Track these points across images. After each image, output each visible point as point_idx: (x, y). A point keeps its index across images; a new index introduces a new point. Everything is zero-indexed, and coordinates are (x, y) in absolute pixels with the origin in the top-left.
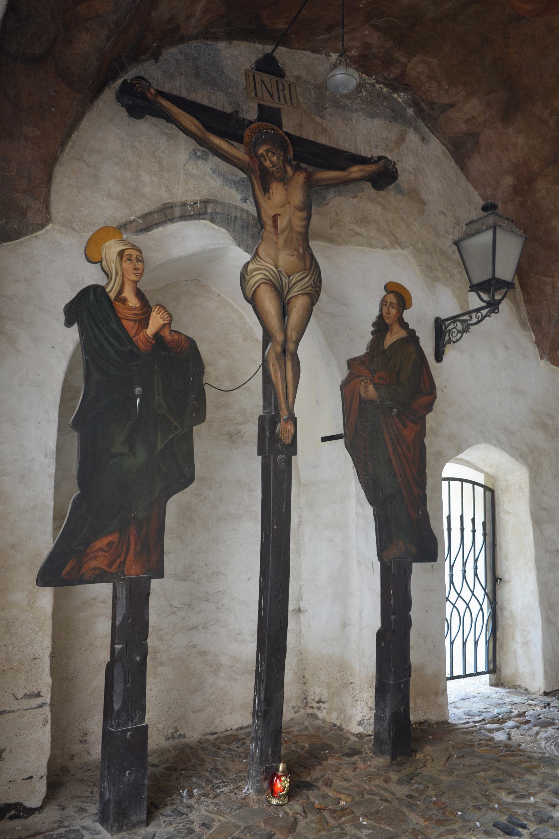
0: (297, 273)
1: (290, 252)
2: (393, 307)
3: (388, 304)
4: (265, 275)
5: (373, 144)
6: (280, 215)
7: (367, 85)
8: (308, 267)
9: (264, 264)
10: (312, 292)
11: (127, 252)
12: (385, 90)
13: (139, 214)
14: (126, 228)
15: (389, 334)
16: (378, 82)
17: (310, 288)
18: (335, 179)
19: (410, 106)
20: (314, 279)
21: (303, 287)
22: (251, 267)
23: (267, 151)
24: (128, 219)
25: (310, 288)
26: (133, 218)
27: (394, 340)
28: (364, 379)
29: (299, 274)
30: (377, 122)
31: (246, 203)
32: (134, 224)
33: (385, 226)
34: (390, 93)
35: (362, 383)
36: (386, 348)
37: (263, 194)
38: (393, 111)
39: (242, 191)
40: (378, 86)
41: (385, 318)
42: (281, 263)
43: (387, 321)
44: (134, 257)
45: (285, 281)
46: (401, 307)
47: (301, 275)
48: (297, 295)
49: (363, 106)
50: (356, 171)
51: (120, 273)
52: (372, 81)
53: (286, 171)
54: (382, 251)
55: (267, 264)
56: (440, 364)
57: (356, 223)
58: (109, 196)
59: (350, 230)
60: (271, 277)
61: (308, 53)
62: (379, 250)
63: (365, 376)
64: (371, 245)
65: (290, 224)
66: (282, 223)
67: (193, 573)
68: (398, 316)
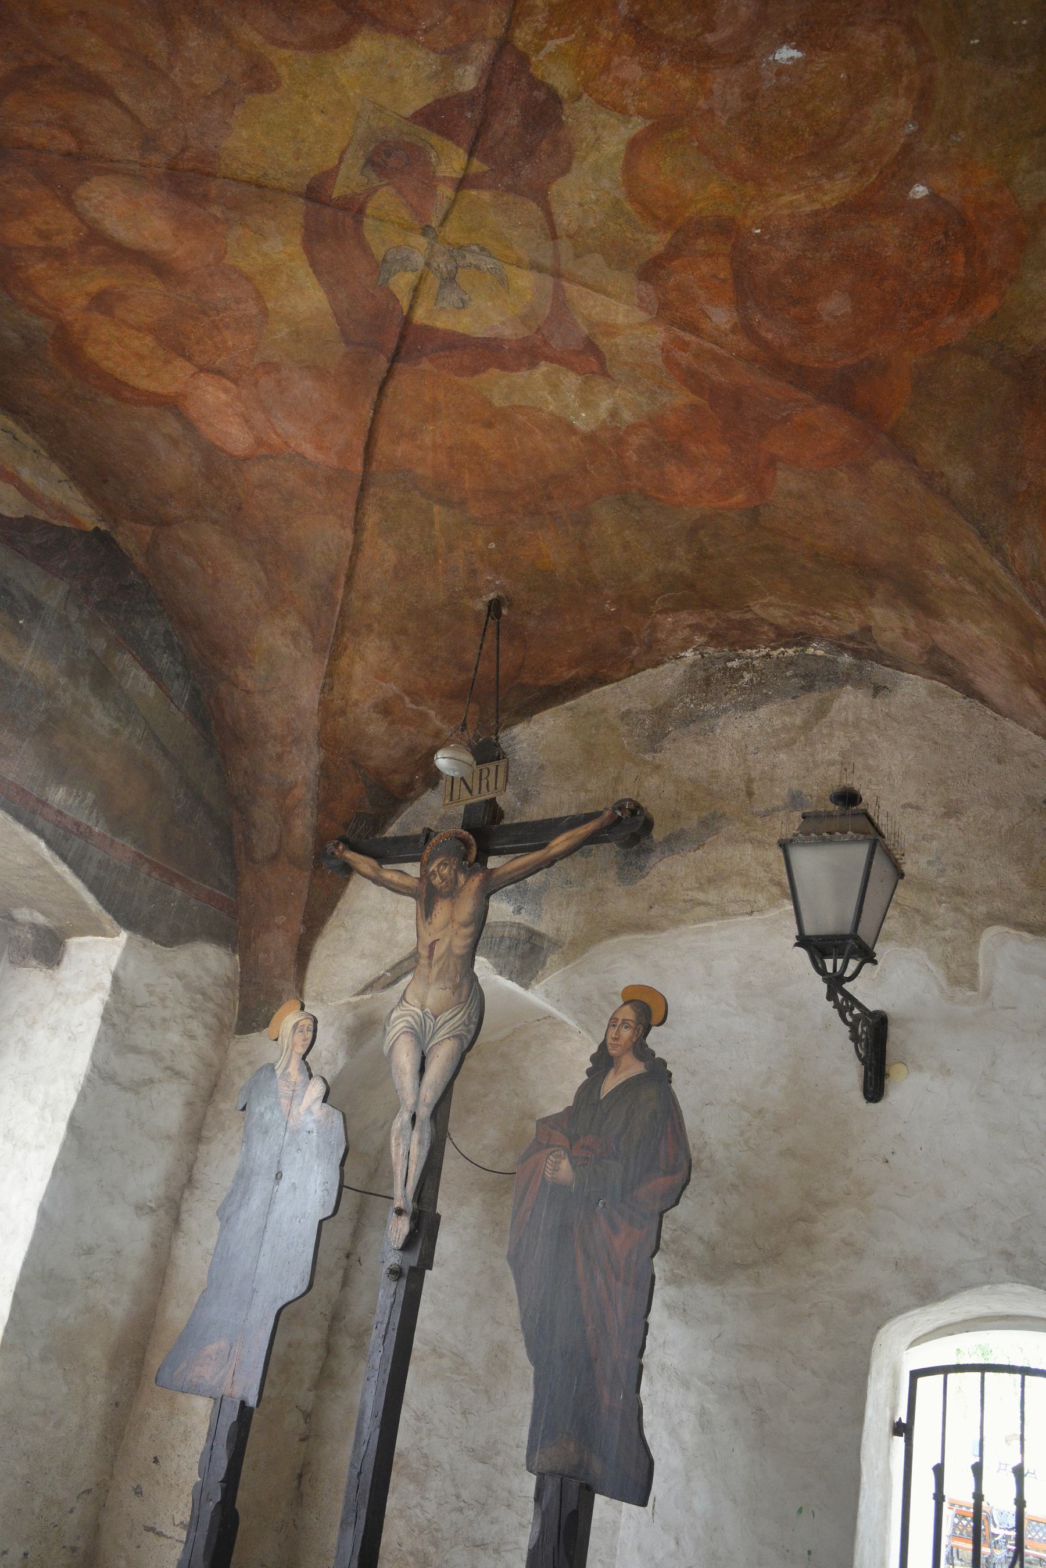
0: (447, 1010)
1: (442, 986)
2: (626, 1028)
3: (620, 1022)
4: (408, 1022)
5: (751, 749)
6: (438, 940)
7: (755, 662)
8: (463, 999)
9: (409, 1009)
10: (463, 1032)
11: (301, 1024)
12: (790, 652)
13: (387, 968)
14: (372, 987)
15: (612, 1071)
16: (774, 649)
17: (461, 1028)
18: (525, 866)
19: (840, 653)
20: (469, 1015)
21: (452, 1028)
22: (394, 1015)
23: (439, 866)
24: (377, 975)
25: (461, 1028)
26: (382, 973)
27: (620, 1082)
28: (554, 1152)
29: (450, 1011)
30: (763, 712)
31: (520, 913)
32: (382, 980)
33: (762, 874)
34: (801, 651)
35: (551, 1157)
36: (602, 1097)
37: (424, 919)
38: (804, 677)
39: (516, 900)
40: (775, 653)
41: (610, 1047)
42: (430, 1001)
43: (613, 1052)
44: (305, 1028)
45: (430, 1026)
46: (641, 1024)
47: (451, 1013)
48: (443, 1040)
49: (740, 699)
50: (559, 843)
51: (290, 1047)
52: (764, 652)
53: (456, 881)
54: (748, 918)
55: (412, 1008)
56: (873, 1106)
57: (698, 888)
58: (363, 956)
59: (685, 901)
60: (414, 1023)
61: (649, 671)
62: (740, 919)
63: (559, 1146)
64: (724, 914)
65: (449, 948)
66: (439, 950)
67: (497, 1454)
68: (634, 1040)
